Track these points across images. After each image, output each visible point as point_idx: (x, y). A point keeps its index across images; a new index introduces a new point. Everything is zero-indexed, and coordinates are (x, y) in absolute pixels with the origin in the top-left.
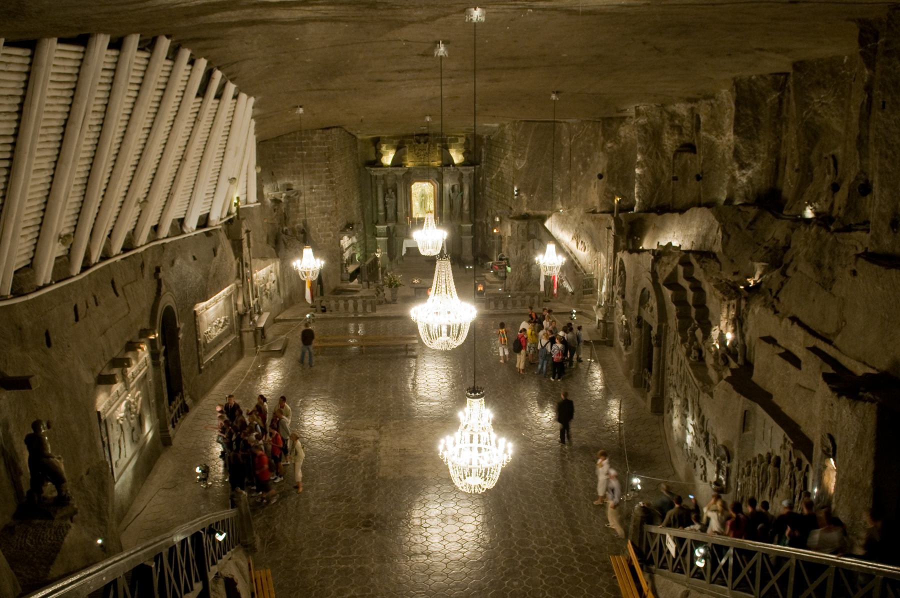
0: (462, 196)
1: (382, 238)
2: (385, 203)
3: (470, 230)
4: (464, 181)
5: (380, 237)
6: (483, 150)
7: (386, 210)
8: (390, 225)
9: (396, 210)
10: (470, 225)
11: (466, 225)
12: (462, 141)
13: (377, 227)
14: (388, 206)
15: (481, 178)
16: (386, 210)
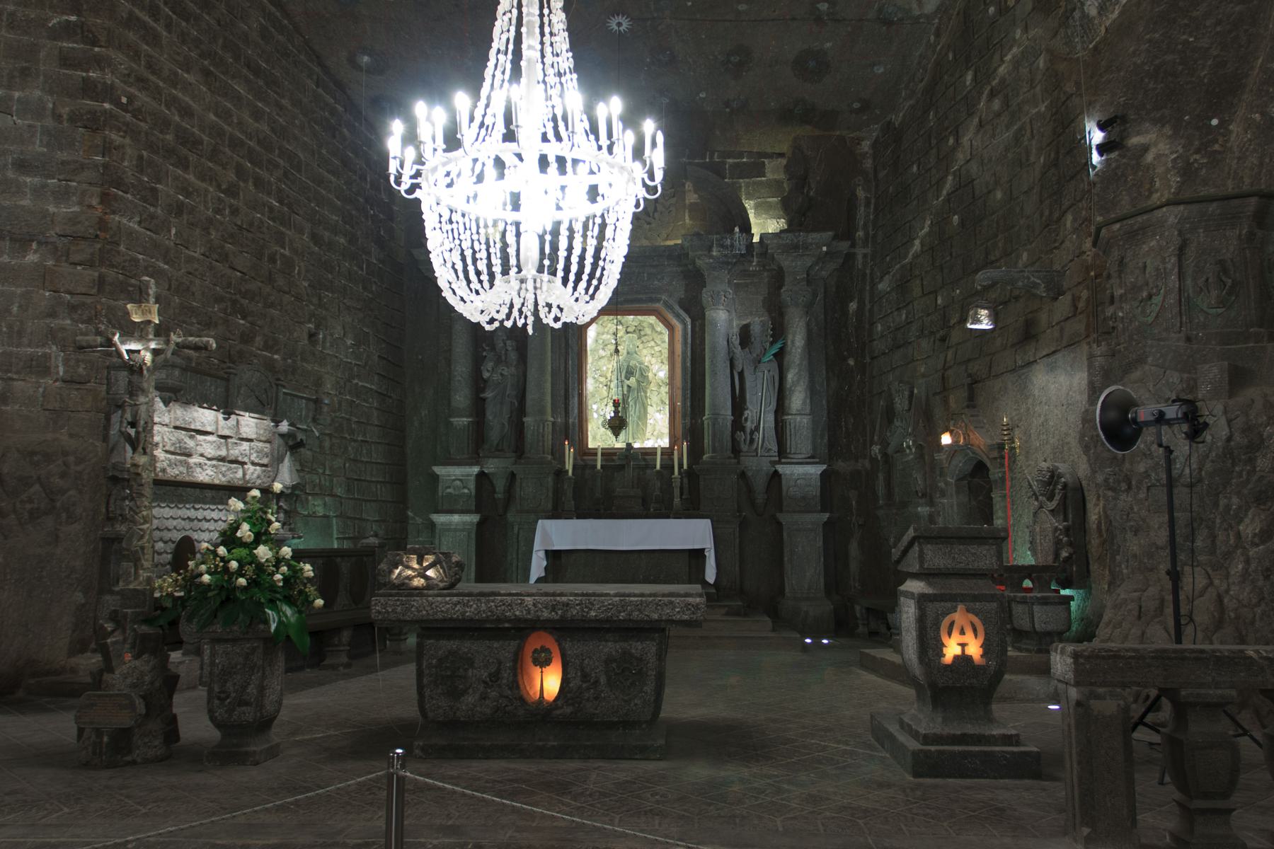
0: (780, 356)
1: (456, 518)
2: (479, 384)
3: (815, 490)
4: (785, 294)
5: (451, 512)
6: (861, 193)
7: (479, 407)
8: (491, 466)
9: (521, 410)
10: (815, 470)
11: (799, 470)
12: (774, 171)
13: (438, 470)
14: (488, 394)
15: (853, 306)
16: (479, 407)
